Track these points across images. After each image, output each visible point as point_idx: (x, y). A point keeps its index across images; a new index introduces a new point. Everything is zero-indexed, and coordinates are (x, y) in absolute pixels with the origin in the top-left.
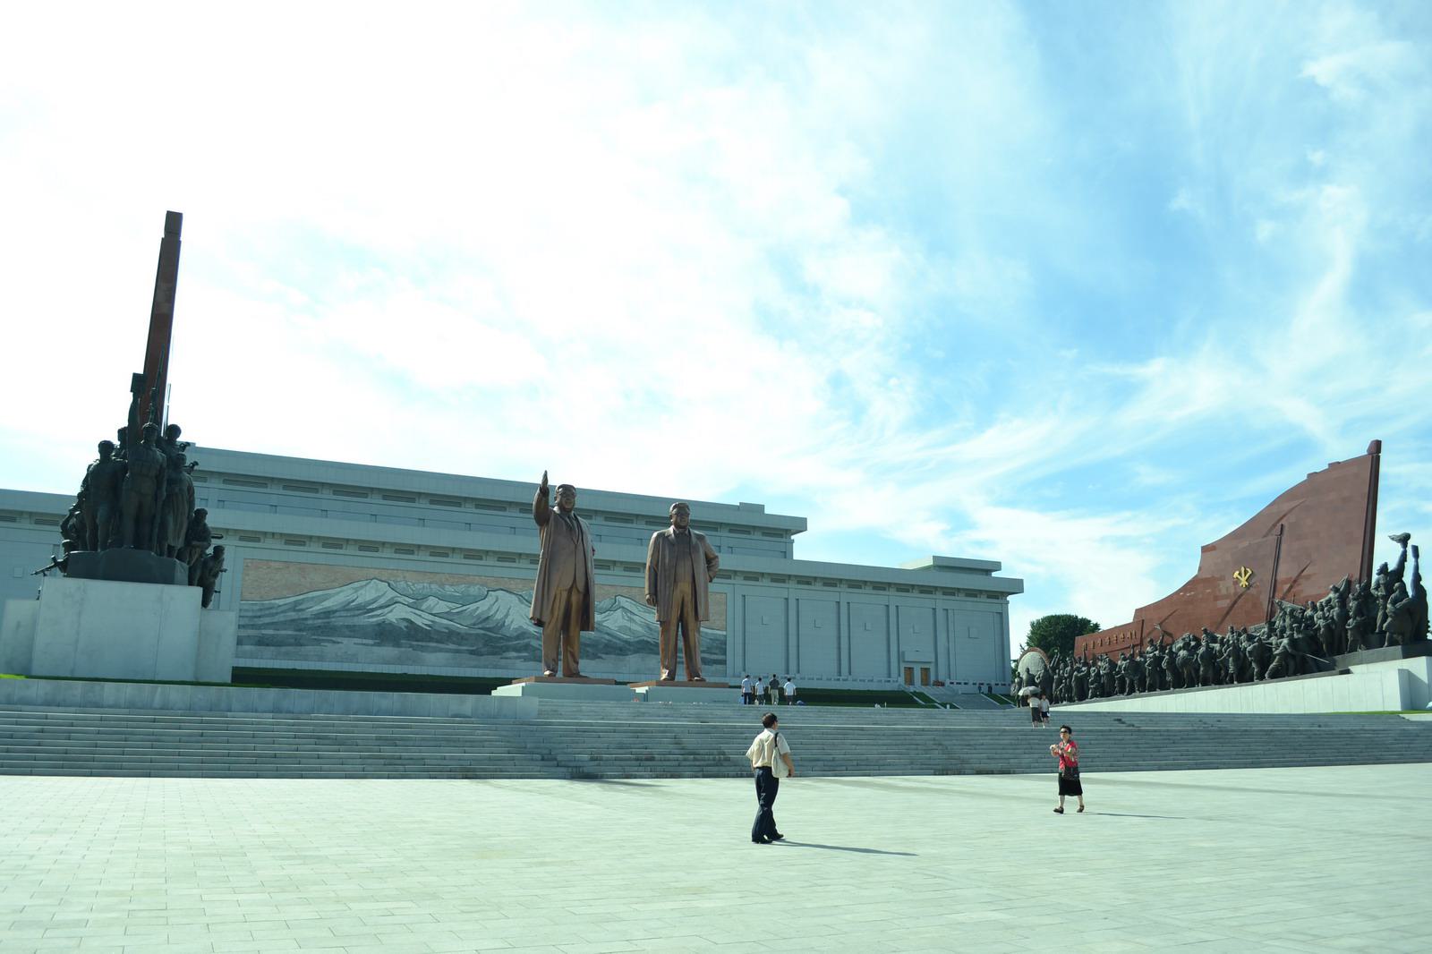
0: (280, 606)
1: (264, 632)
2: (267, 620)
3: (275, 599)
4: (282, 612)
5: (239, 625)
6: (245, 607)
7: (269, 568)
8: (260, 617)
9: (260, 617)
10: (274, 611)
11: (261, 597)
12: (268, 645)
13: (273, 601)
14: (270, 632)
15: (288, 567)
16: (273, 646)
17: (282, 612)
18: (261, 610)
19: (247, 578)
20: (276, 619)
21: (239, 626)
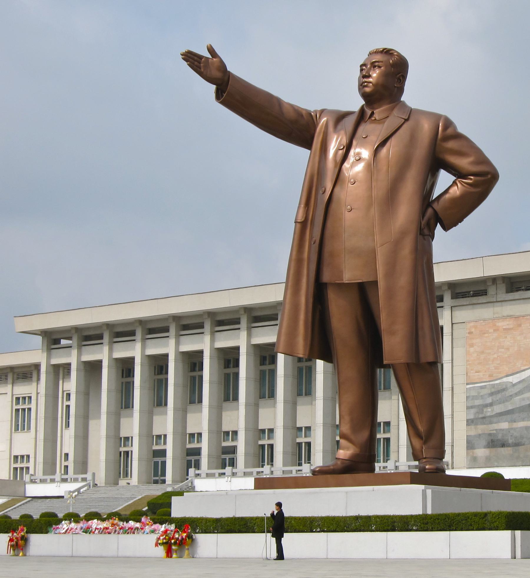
0: (514, 385)
1: (495, 426)
2: (498, 409)
3: (507, 376)
4: (517, 394)
5: (467, 421)
6: (473, 393)
7: (495, 330)
8: (491, 405)
9: (491, 405)
10: (508, 393)
11: (490, 376)
12: (503, 446)
13: (505, 380)
14: (504, 425)
15: (520, 325)
16: (509, 446)
17: (517, 394)
18: (492, 394)
19: (472, 350)
20: (509, 406)
21: (469, 422)
